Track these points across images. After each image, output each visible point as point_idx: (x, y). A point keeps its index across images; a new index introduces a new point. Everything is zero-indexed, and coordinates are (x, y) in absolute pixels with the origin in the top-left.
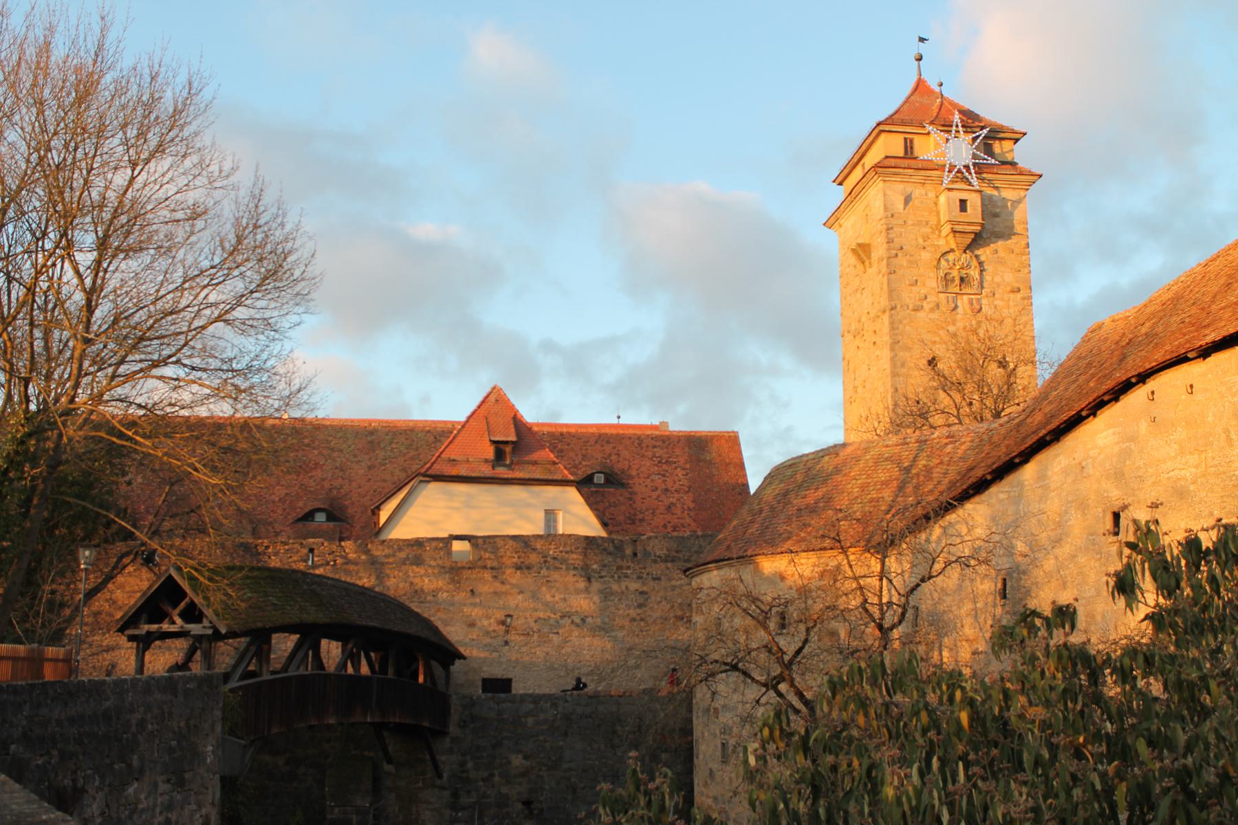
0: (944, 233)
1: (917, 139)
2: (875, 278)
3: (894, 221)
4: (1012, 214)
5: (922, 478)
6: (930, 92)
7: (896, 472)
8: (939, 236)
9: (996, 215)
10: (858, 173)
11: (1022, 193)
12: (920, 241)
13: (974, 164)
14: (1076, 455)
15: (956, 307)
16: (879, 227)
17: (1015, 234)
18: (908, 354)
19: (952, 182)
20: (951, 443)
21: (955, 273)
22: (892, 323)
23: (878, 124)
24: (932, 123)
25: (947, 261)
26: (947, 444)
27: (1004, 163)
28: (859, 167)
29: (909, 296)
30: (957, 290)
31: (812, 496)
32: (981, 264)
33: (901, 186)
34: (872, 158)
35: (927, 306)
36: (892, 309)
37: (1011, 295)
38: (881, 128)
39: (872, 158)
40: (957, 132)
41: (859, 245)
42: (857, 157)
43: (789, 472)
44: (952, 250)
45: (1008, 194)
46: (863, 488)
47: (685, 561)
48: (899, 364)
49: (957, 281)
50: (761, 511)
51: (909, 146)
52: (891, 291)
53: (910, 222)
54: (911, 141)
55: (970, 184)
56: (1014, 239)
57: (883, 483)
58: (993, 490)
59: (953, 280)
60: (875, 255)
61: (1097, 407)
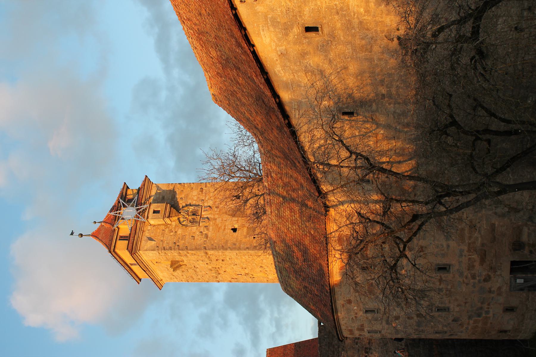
0: (169, 222)
1: (121, 234)
2: (188, 258)
3: (161, 246)
4: (164, 191)
5: (289, 188)
6: (99, 230)
7: (286, 205)
8: (170, 225)
9: (163, 198)
10: (136, 269)
11: (154, 185)
12: (172, 234)
13: (139, 213)
14: (275, 59)
15: (207, 218)
16: (163, 254)
17: (174, 189)
18: (229, 242)
19: (144, 217)
20: (271, 174)
21: (190, 218)
22: (213, 249)
23: (110, 252)
24: (113, 226)
25: (184, 221)
26: (271, 177)
27: (138, 193)
28: (133, 267)
29: (200, 240)
30: (199, 217)
31: (298, 254)
32: (187, 205)
33: (143, 242)
34: (129, 259)
35: (206, 232)
36: (205, 249)
37: (204, 191)
38: (112, 251)
39: (129, 259)
40: (119, 213)
41: (171, 267)
42: (126, 267)
43: (284, 273)
44: (179, 219)
45: (153, 192)
46: (293, 223)
47: (334, 354)
48: (234, 246)
49: (194, 217)
50: (305, 287)
51: (123, 238)
52: (196, 249)
53: (162, 238)
54: (121, 237)
55: (146, 209)
56: (176, 190)
57: (291, 212)
58: (294, 122)
59: (194, 219)
60: (178, 258)
61: (247, 38)
